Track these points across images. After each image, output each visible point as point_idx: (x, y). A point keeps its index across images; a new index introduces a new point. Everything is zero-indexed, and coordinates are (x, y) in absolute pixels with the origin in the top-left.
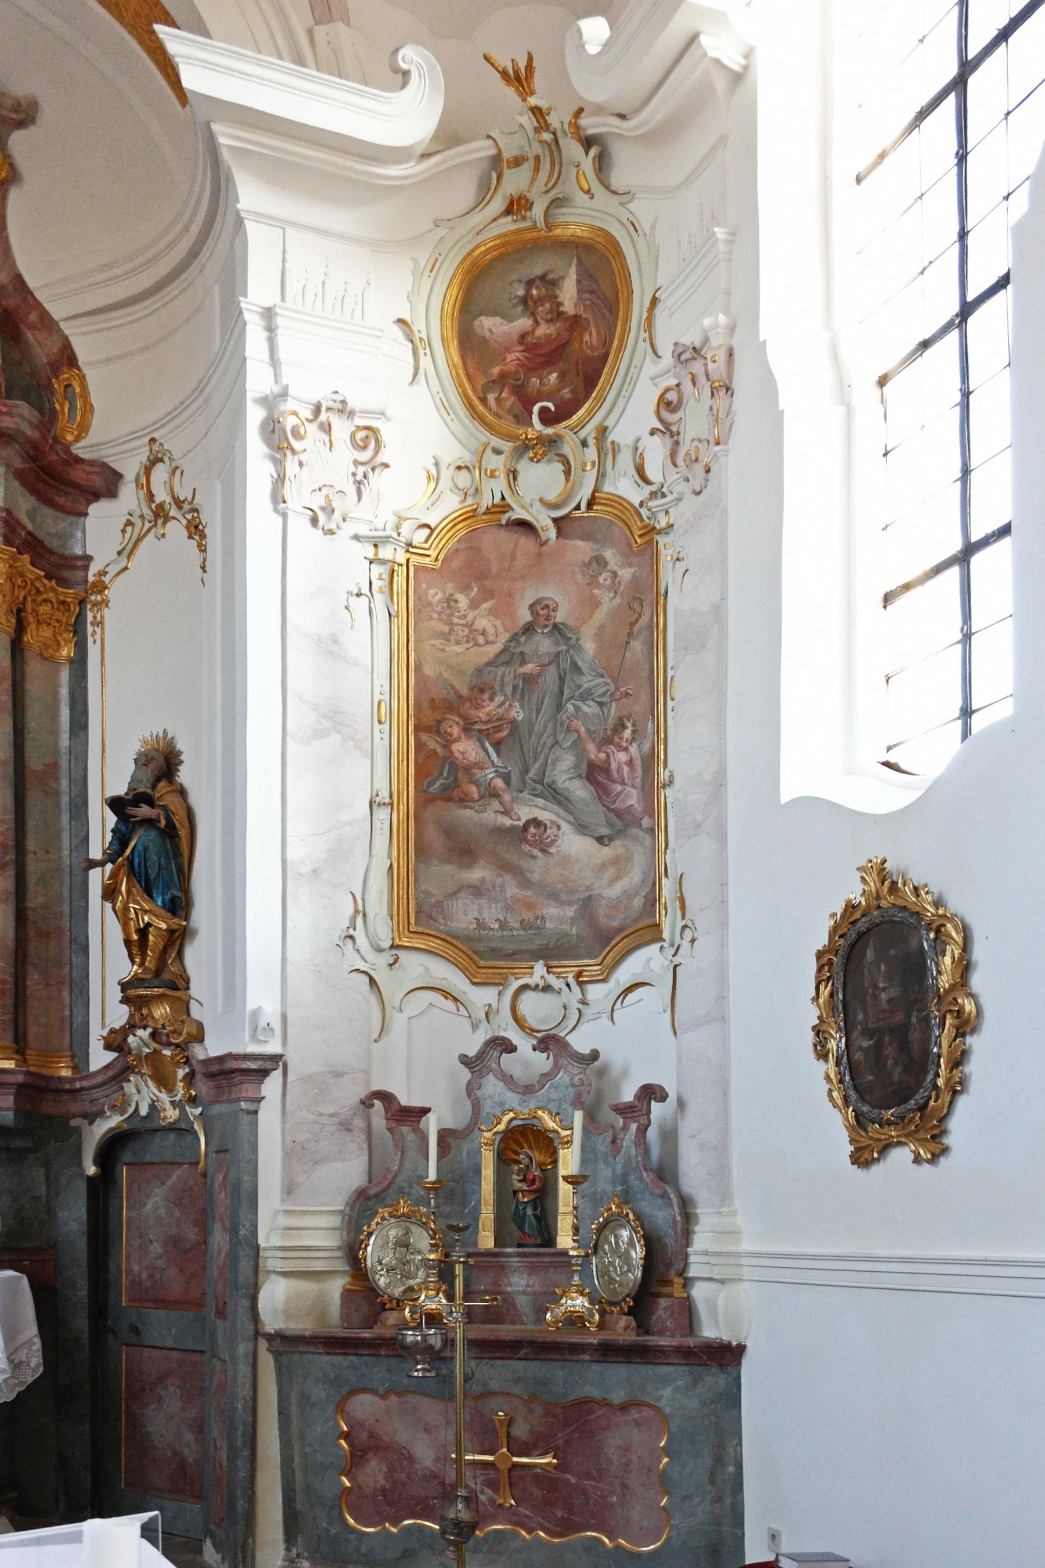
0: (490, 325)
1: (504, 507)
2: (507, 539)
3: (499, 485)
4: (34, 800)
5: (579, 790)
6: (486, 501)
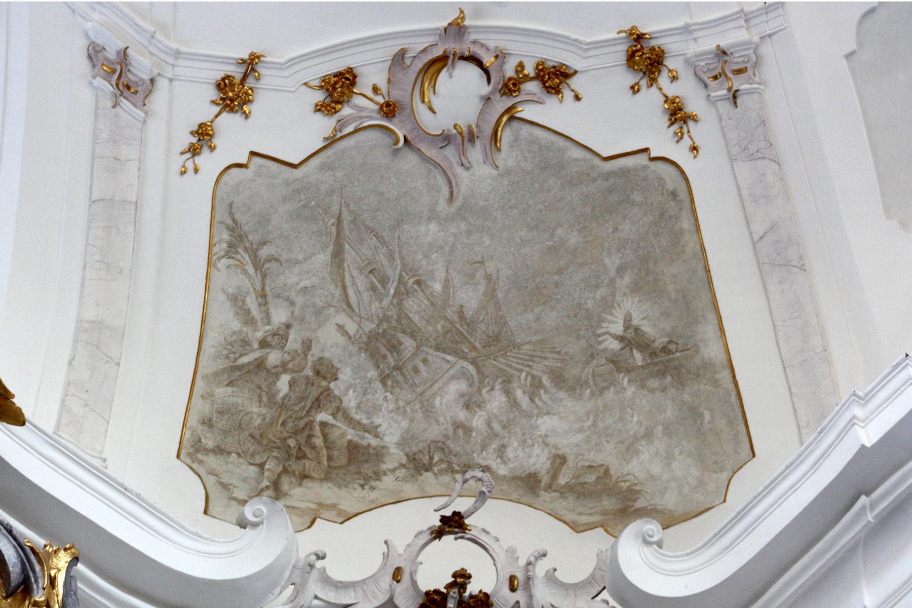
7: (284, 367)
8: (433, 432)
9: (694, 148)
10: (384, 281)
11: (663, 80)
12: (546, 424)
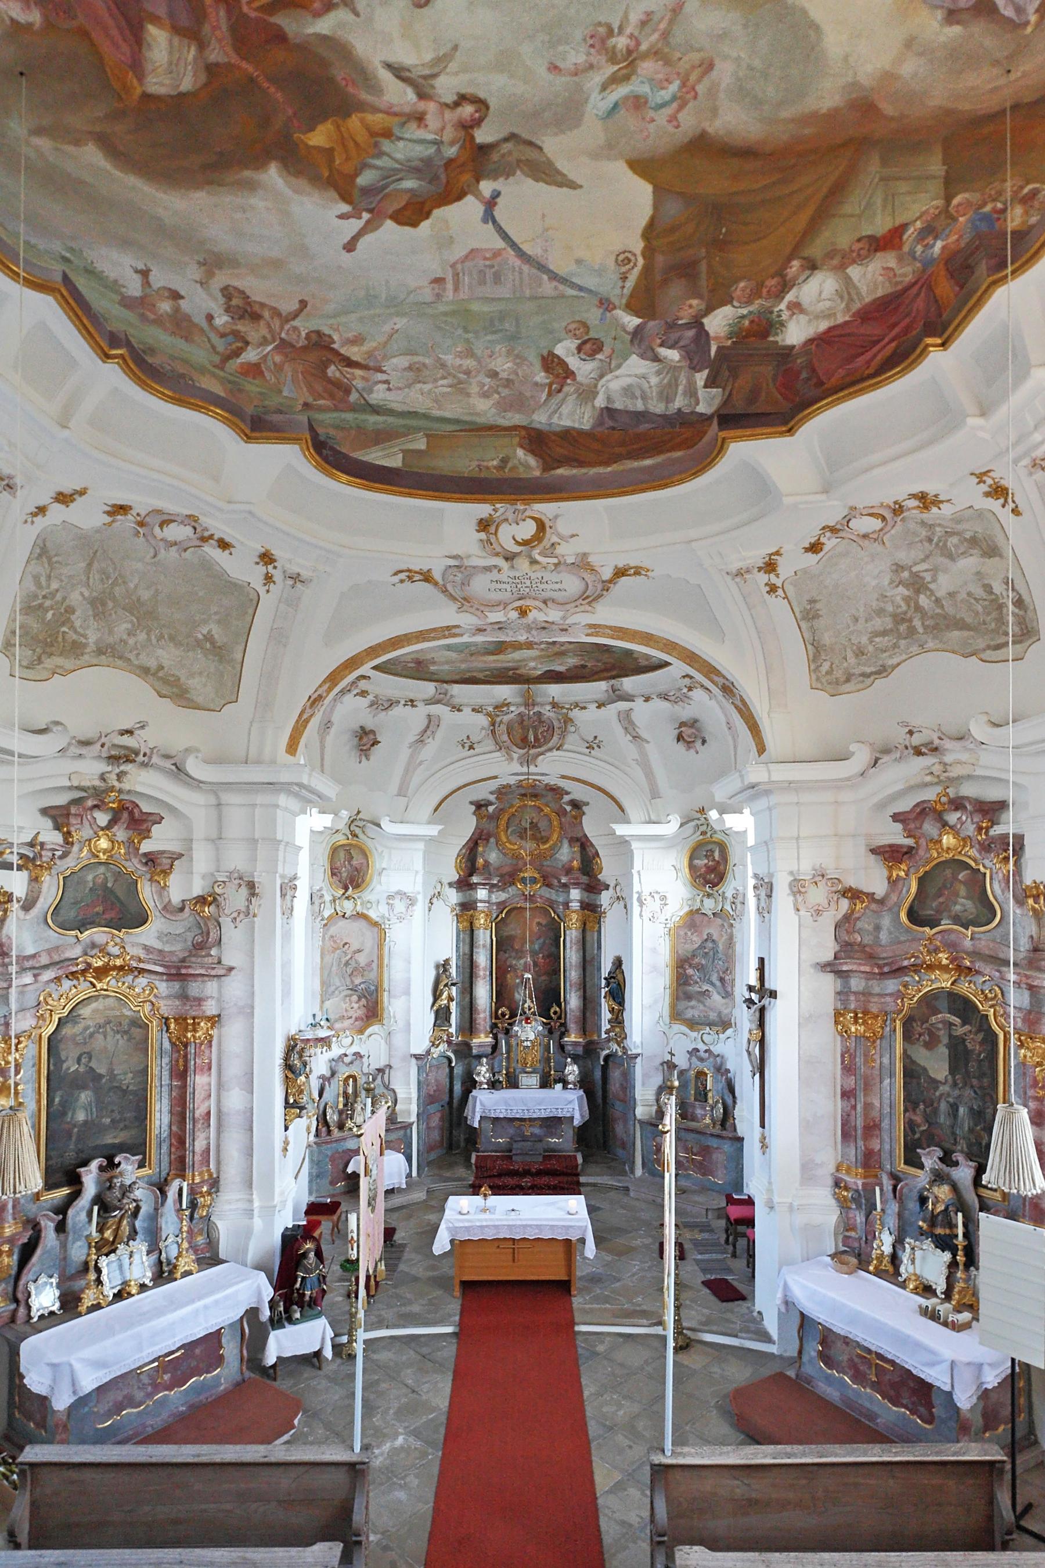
0: (697, 862)
3: (699, 904)
4: (589, 968)
8: (111, 640)
10: (108, 578)
12: (160, 652)
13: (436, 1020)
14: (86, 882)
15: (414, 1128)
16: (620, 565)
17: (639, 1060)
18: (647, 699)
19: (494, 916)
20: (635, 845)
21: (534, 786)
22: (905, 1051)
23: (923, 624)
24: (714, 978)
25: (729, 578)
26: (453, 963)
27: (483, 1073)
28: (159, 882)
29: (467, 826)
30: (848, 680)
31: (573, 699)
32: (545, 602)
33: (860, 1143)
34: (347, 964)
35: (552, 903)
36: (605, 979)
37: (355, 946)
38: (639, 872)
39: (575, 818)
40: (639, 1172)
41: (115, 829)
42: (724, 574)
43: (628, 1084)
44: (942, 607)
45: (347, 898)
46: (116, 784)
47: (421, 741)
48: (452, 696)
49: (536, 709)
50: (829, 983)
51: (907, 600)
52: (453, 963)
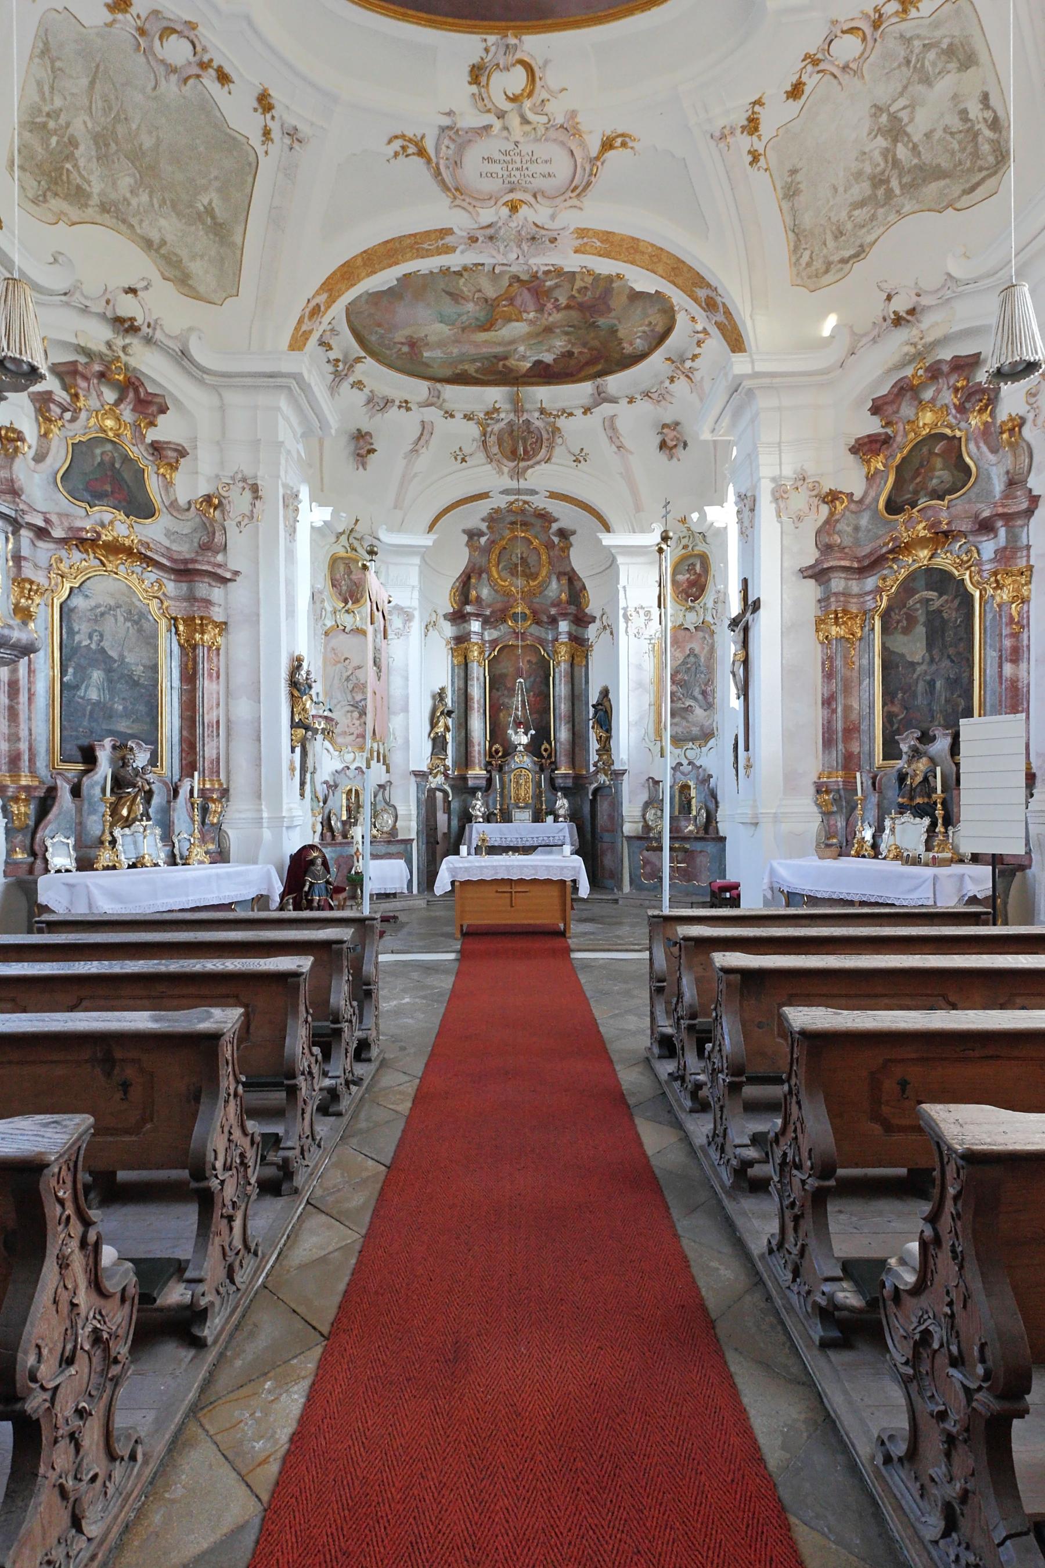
0: (680, 578)
1: (682, 625)
2: (682, 633)
4: (576, 702)
5: (700, 697)
6: (678, 624)
7: (55, 132)
8: (113, 196)
9: (266, 153)
11: (268, 116)
12: (163, 222)
13: (433, 749)
14: (93, 456)
15: (415, 844)
16: (608, 133)
17: (625, 777)
18: (631, 400)
19: (487, 654)
20: (620, 560)
21: (523, 511)
22: (883, 644)
23: (900, 183)
24: (697, 693)
25: (712, 143)
26: (449, 692)
27: (478, 807)
28: (164, 476)
29: (459, 560)
30: (827, 271)
31: (560, 405)
32: (535, 196)
33: (840, 746)
34: (348, 679)
35: (542, 642)
36: (593, 706)
37: (355, 662)
38: (624, 587)
39: (563, 550)
40: (627, 888)
41: (122, 406)
42: (708, 136)
43: (616, 805)
44: (919, 155)
45: (347, 611)
46: (121, 354)
47: (414, 451)
48: (444, 401)
49: (525, 416)
50: (811, 589)
51: (885, 153)
52: (449, 692)
